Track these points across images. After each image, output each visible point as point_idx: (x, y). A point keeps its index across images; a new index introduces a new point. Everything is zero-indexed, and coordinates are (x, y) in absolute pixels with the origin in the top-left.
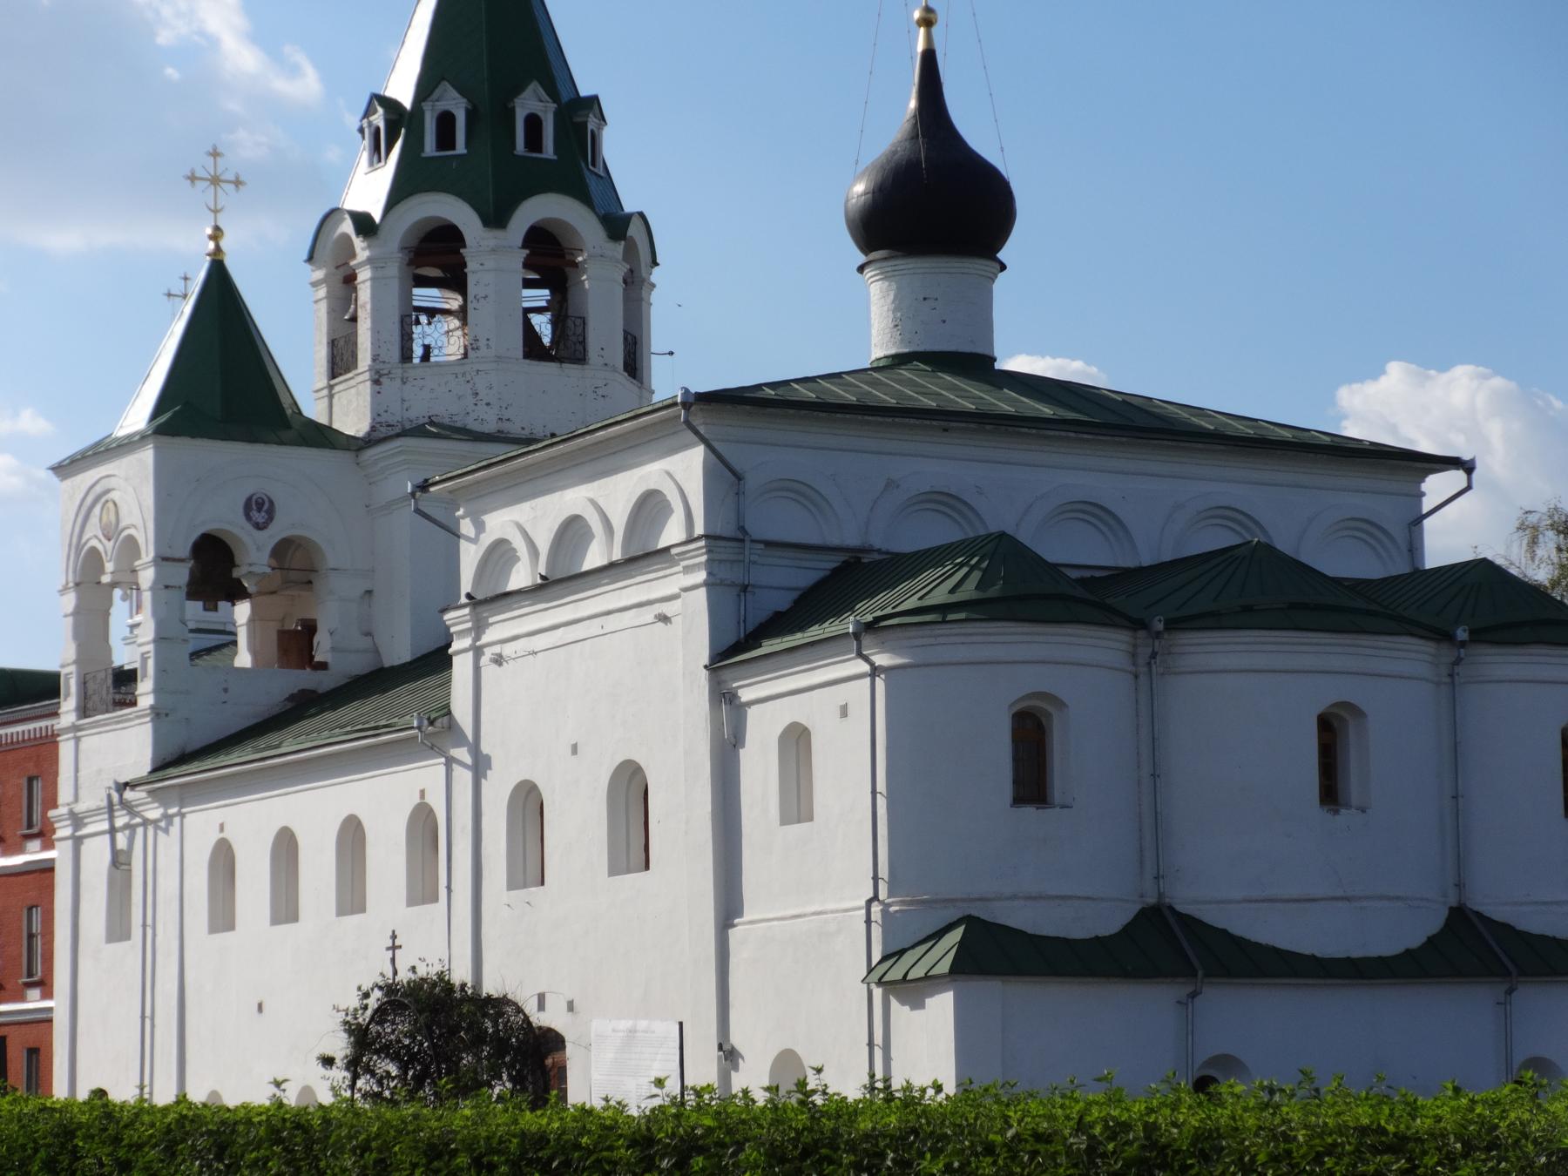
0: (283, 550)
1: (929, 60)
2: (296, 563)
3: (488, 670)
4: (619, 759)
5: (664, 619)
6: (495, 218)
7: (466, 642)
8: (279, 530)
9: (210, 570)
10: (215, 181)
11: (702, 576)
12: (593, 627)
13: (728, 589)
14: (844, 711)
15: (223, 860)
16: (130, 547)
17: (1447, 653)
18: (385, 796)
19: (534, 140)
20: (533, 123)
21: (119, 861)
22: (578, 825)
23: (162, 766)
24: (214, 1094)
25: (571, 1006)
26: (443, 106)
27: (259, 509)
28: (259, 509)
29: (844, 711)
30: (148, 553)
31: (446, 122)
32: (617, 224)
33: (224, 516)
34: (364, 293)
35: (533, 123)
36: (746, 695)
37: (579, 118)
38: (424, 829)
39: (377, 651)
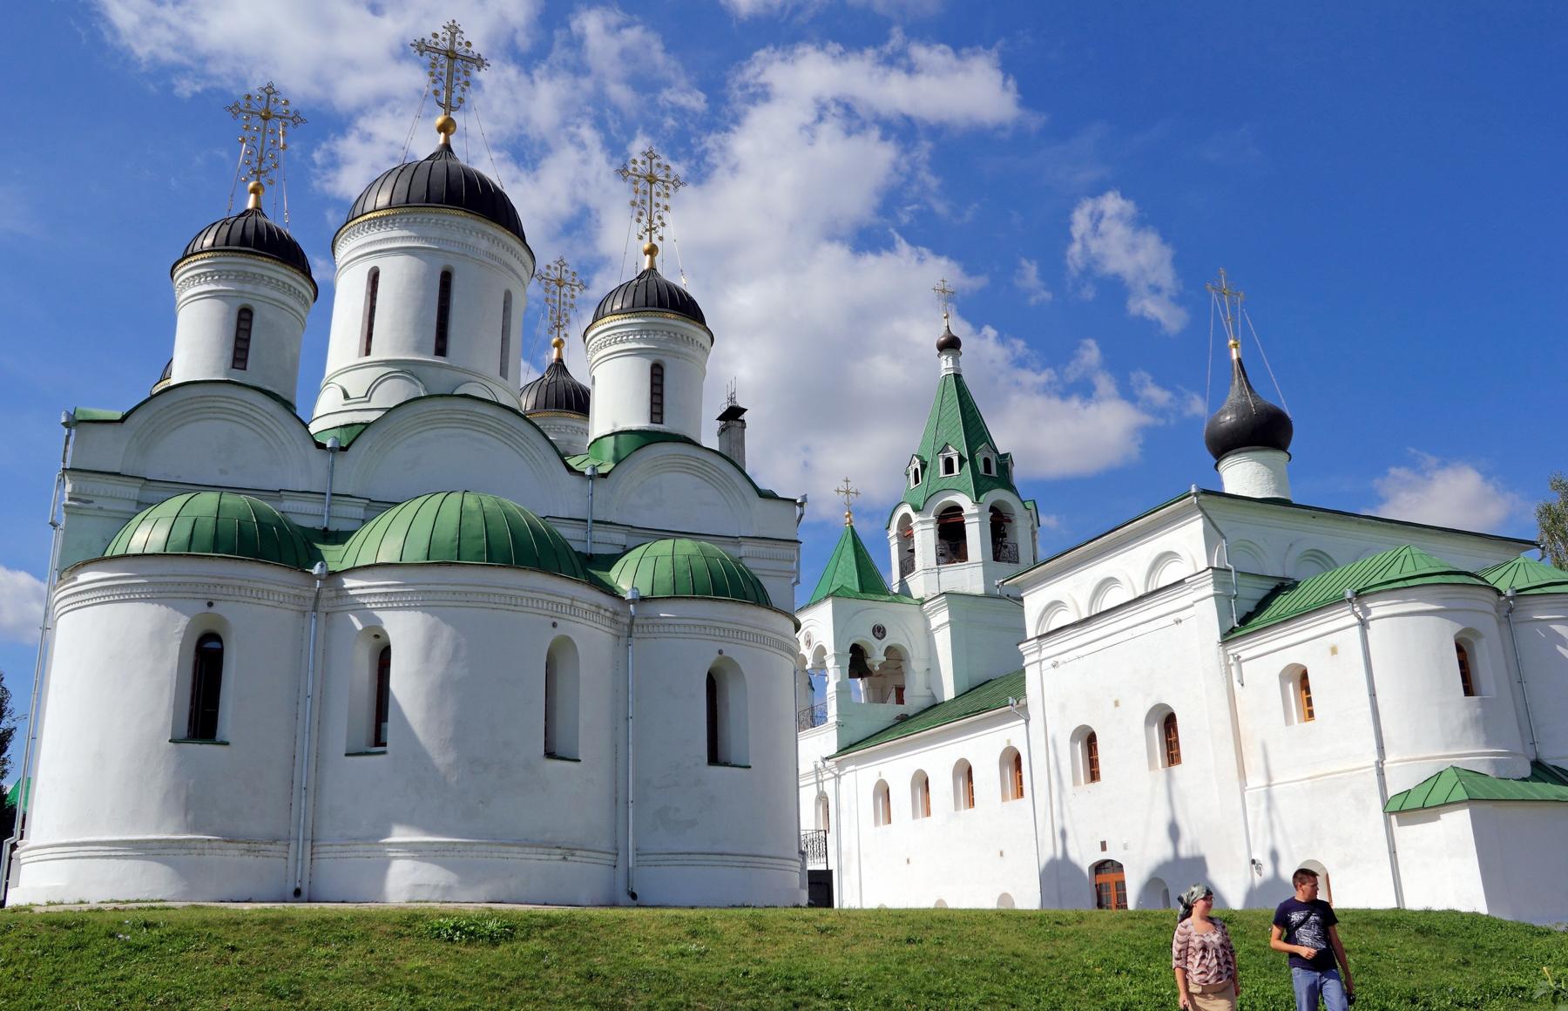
0: (889, 650)
2: (896, 656)
3: (1050, 674)
4: (1149, 706)
5: (1178, 622)
7: (1035, 657)
8: (889, 640)
9: (858, 662)
11: (1210, 590)
12: (1126, 635)
13: (1223, 599)
14: (1334, 651)
15: (883, 792)
16: (821, 651)
18: (982, 747)
20: (987, 462)
21: (822, 799)
23: (844, 749)
24: (1004, 897)
25: (1125, 847)
28: (879, 632)
29: (1334, 651)
30: (830, 650)
33: (865, 637)
34: (917, 537)
36: (1244, 655)
38: (1013, 761)
39: (933, 696)
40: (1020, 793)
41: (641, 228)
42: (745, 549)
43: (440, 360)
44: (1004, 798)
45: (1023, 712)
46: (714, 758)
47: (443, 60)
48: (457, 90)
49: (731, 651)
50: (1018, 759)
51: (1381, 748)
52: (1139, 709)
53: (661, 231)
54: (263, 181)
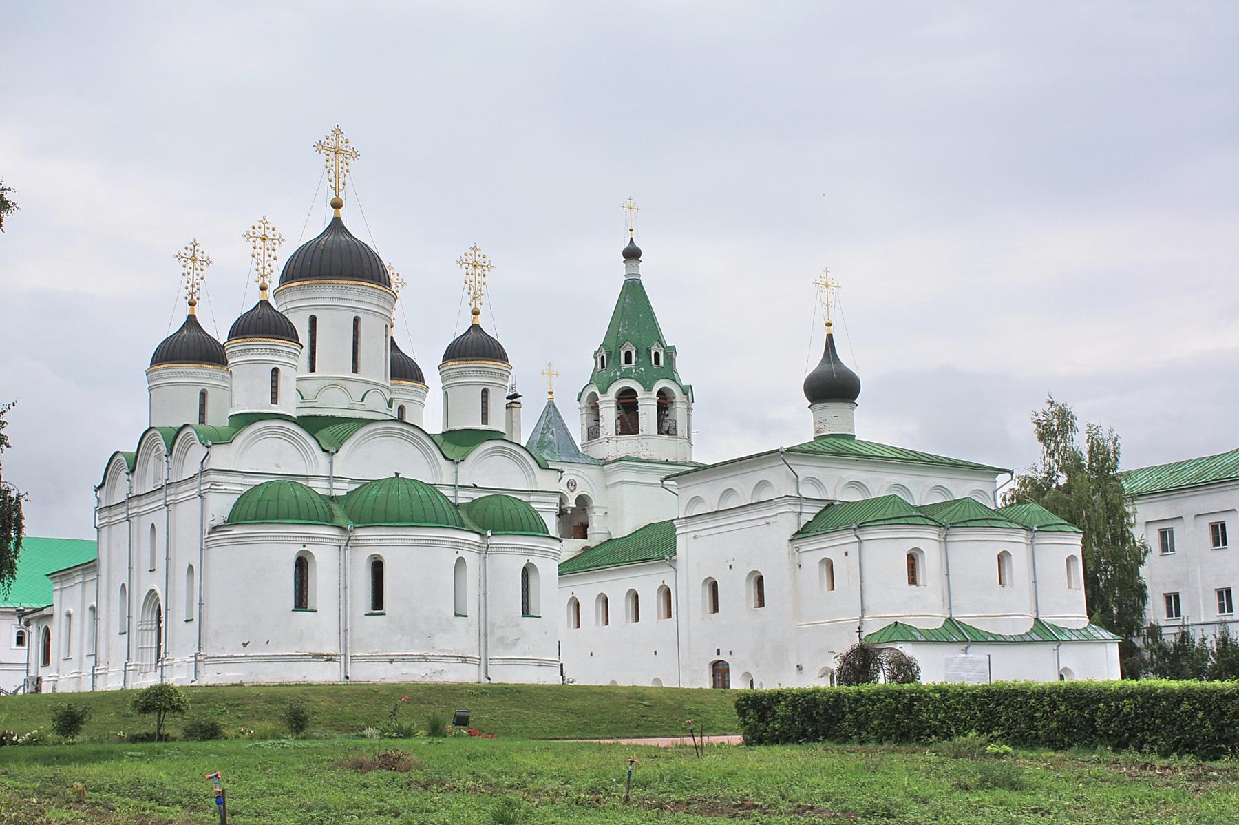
1: (830, 338)
6: (648, 389)
10: (550, 374)
12: (739, 526)
14: (846, 554)
17: (1030, 535)
18: (647, 582)
19: (657, 362)
20: (657, 355)
22: (736, 592)
26: (628, 348)
27: (572, 484)
28: (572, 484)
29: (846, 554)
31: (628, 355)
32: (687, 391)
35: (657, 355)
37: (670, 353)
40: (669, 616)
41: (469, 298)
42: (533, 498)
43: (355, 376)
44: (659, 617)
45: (672, 563)
46: (526, 612)
47: (333, 155)
48: (342, 176)
49: (533, 560)
50: (669, 592)
51: (863, 610)
52: (742, 572)
53: (483, 299)
54: (267, 281)
